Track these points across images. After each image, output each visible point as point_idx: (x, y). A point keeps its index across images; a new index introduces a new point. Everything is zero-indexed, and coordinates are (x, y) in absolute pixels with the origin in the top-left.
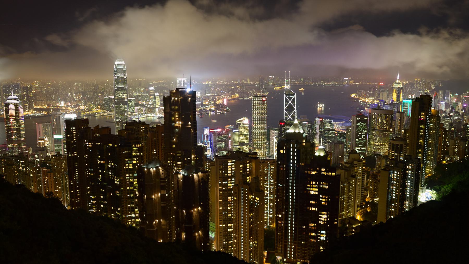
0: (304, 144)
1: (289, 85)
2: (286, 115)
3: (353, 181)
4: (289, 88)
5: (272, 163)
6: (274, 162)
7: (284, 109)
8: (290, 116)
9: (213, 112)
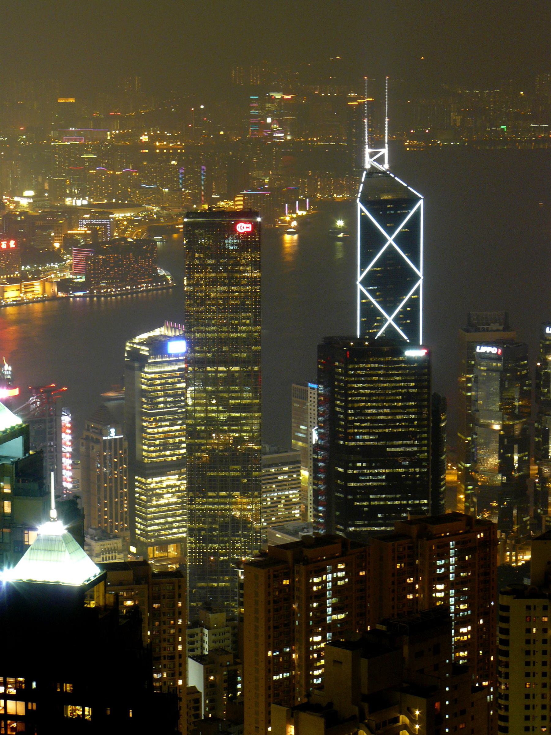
0: (7, 507)
1: (385, 151)
2: (368, 309)
3: (417, 713)
4: (386, 166)
5: (130, 584)
6: (137, 581)
7: (356, 279)
8: (390, 313)
9: (81, 294)
